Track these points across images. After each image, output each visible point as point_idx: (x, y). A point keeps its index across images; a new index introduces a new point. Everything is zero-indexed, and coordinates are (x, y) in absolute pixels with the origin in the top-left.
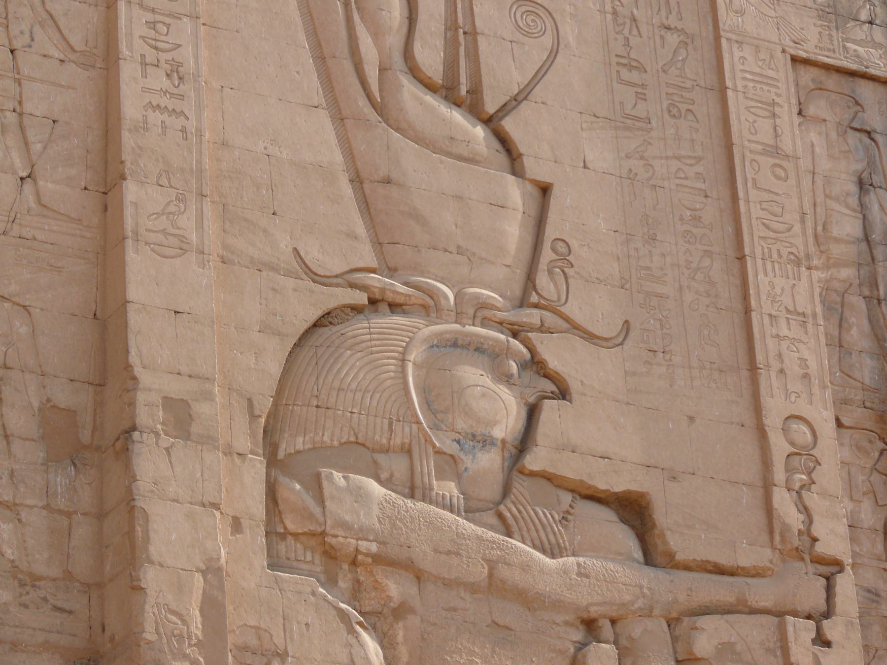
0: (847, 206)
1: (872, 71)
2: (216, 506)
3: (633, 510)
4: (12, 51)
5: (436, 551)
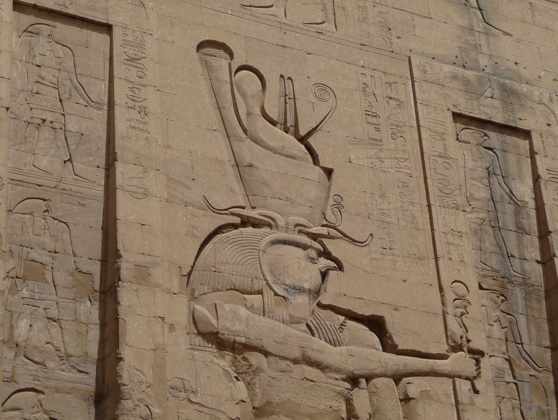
0: (482, 184)
4: (61, 101)
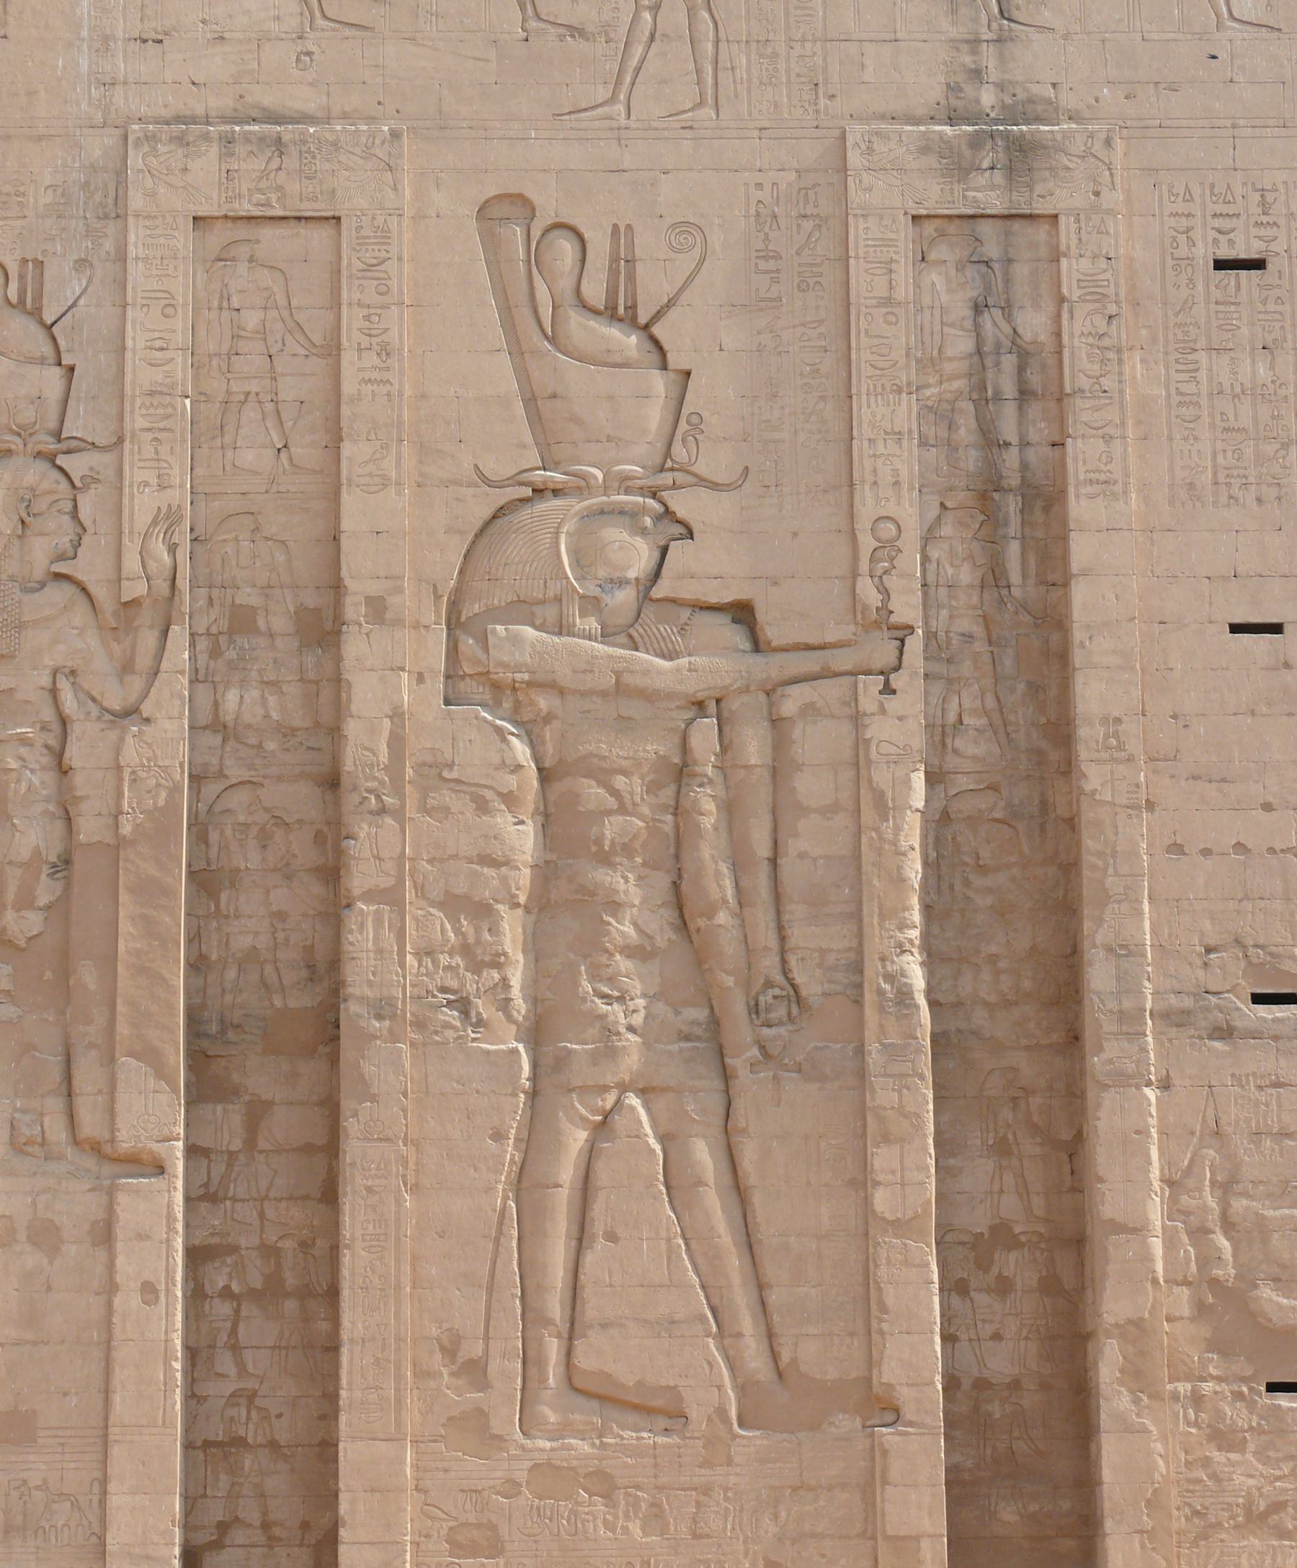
0: (963, 329)
1: (989, 211)
2: (403, 669)
3: (742, 613)
5: (575, 672)
